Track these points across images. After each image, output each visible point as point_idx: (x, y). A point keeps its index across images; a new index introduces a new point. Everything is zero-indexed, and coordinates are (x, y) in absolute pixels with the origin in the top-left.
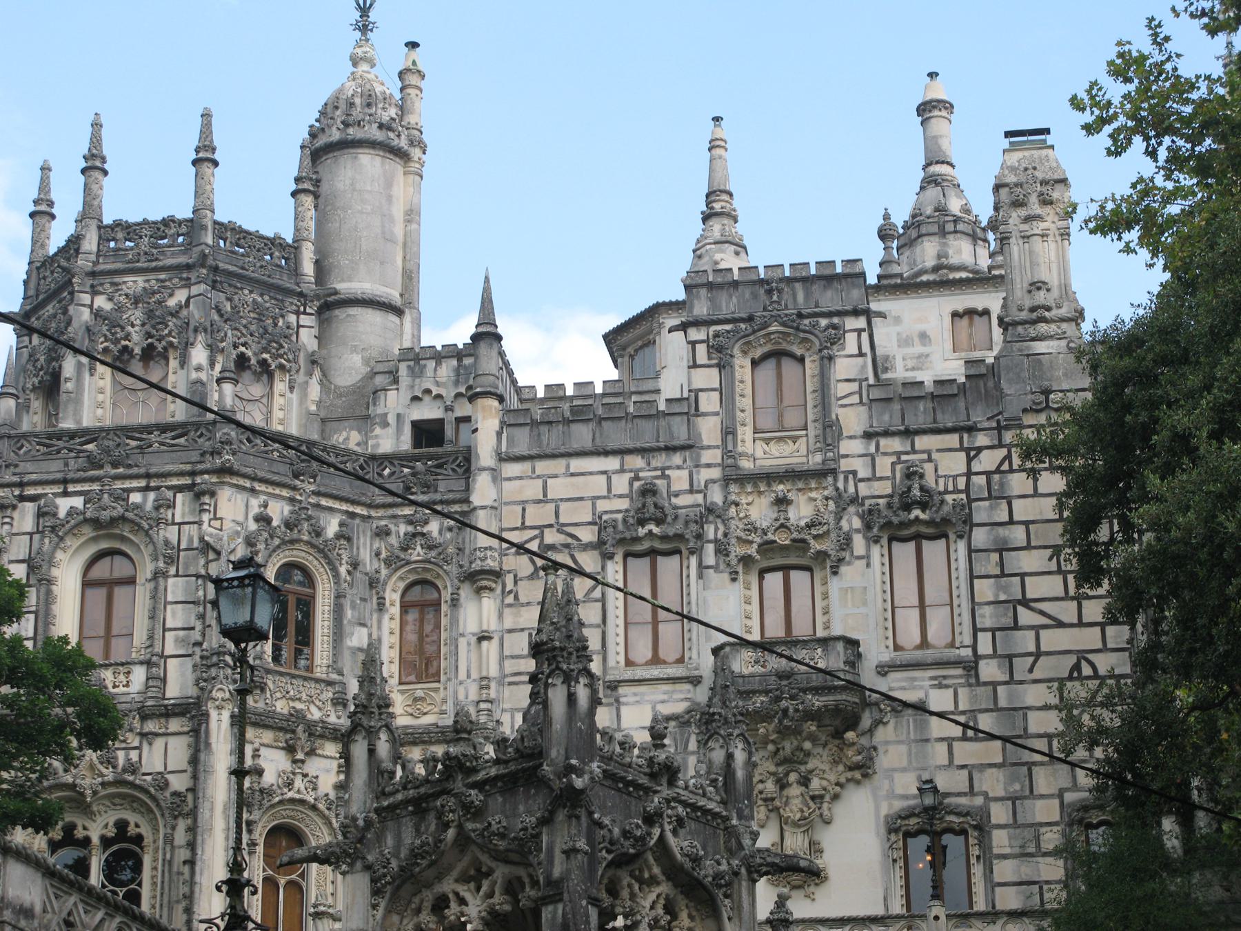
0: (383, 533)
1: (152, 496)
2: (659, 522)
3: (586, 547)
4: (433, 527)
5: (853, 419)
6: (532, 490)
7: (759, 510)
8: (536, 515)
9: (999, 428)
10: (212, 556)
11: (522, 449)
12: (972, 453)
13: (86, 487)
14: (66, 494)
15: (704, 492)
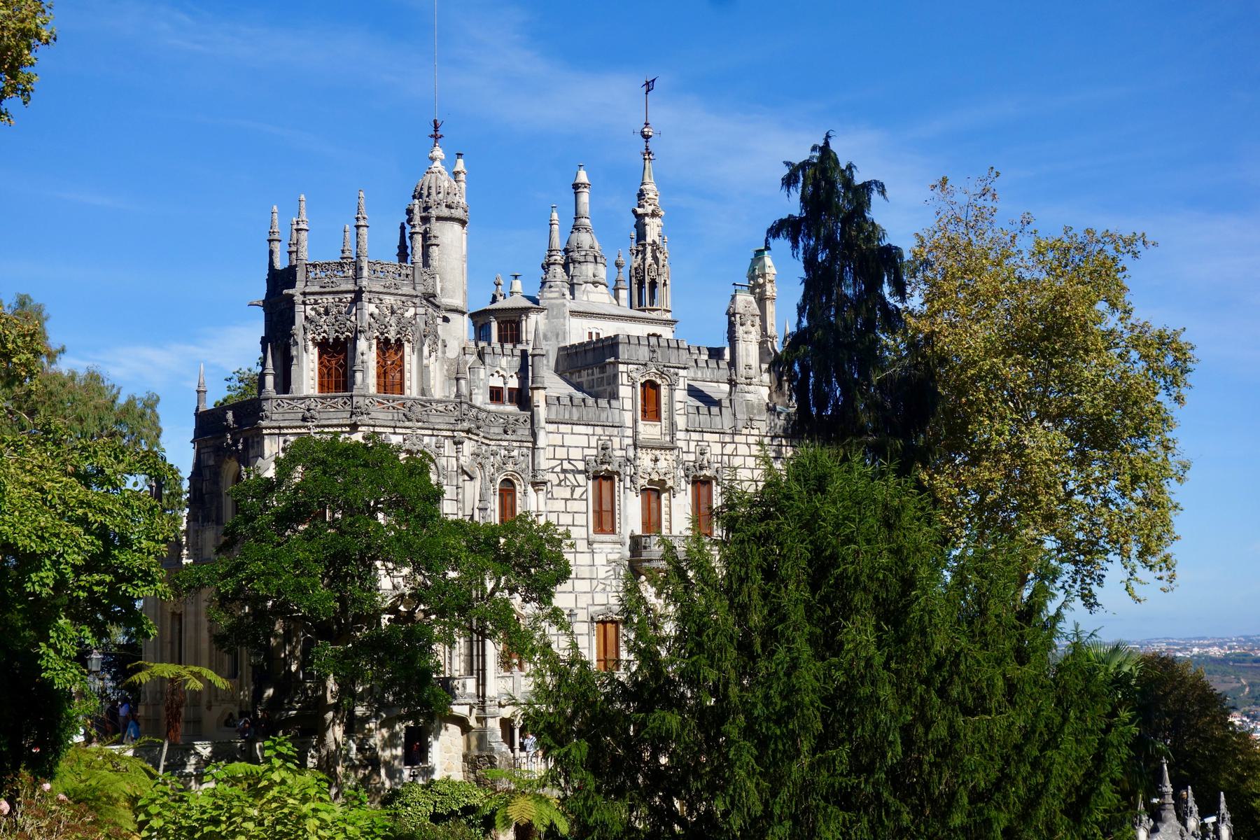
0: (494, 454)
1: (434, 439)
2: (609, 463)
3: (580, 472)
4: (515, 453)
5: (681, 422)
6: (557, 439)
7: (645, 459)
8: (561, 453)
9: (733, 434)
10: (466, 478)
11: (553, 417)
12: (724, 444)
13: (404, 431)
14: (395, 433)
15: (626, 450)
